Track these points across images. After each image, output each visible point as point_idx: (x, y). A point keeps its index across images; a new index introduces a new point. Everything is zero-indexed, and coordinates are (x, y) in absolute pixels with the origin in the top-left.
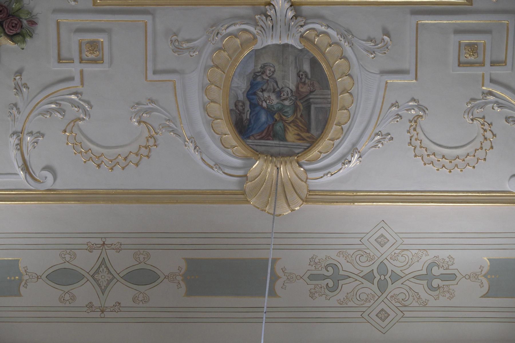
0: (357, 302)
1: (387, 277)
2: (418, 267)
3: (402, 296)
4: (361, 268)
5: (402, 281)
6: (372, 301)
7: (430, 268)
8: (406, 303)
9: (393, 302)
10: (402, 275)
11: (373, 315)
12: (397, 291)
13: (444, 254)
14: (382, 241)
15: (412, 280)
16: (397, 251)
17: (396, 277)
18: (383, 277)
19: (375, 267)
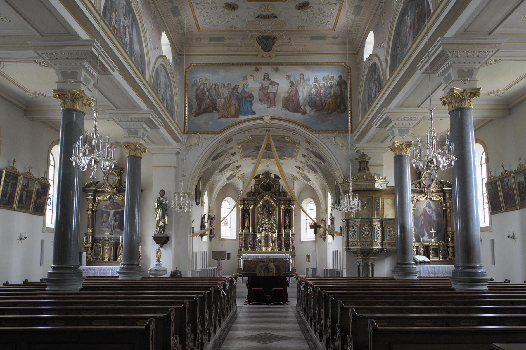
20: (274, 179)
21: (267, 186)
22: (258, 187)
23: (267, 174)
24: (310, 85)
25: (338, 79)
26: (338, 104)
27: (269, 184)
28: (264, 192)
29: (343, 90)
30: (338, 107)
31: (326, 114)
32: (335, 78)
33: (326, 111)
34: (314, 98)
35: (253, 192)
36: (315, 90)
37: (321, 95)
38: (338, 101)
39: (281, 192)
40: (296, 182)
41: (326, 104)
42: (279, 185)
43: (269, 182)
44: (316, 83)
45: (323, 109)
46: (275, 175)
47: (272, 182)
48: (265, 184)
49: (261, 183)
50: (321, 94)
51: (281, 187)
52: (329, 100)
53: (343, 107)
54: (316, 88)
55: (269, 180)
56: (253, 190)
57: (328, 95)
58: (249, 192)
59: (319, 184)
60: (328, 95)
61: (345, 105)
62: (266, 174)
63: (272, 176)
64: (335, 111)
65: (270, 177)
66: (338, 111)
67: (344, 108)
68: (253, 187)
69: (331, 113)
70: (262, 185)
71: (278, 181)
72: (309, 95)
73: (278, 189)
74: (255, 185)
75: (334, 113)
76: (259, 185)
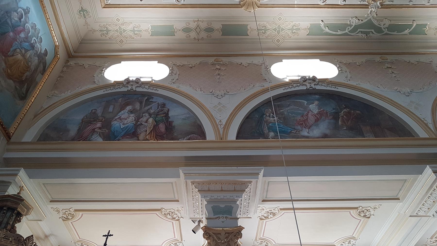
0: (271, 37)
1: (280, 30)
2: (290, 27)
3: (284, 35)
4: (273, 27)
5: (284, 30)
6: (275, 37)
7: (293, 27)
8: (285, 37)
9: (281, 37)
10: (285, 29)
11: (275, 41)
12: (283, 34)
13: (297, 23)
14: (280, 19)
15: (288, 30)
16: (284, 22)
17: (283, 29)
18: (279, 30)
19: (277, 27)
24: (17, 4)
25: (43, 52)
26: (24, 78)
29: (39, 70)
30: (21, 82)
31: (3, 69)
32: (42, 43)
33: (6, 64)
34: (8, 24)
36: (16, 19)
37: (18, 37)
38: (26, 74)
41: (13, 55)
44: (25, 14)
45: (5, 56)
50: (19, 34)
52: (19, 57)
53: (24, 90)
54: (20, 19)
57: (23, 51)
60: (23, 51)
61: (28, 90)
64: (14, 81)
66: (18, 87)
67: (24, 93)
69: (10, 77)
72: (7, 12)
75: (11, 81)
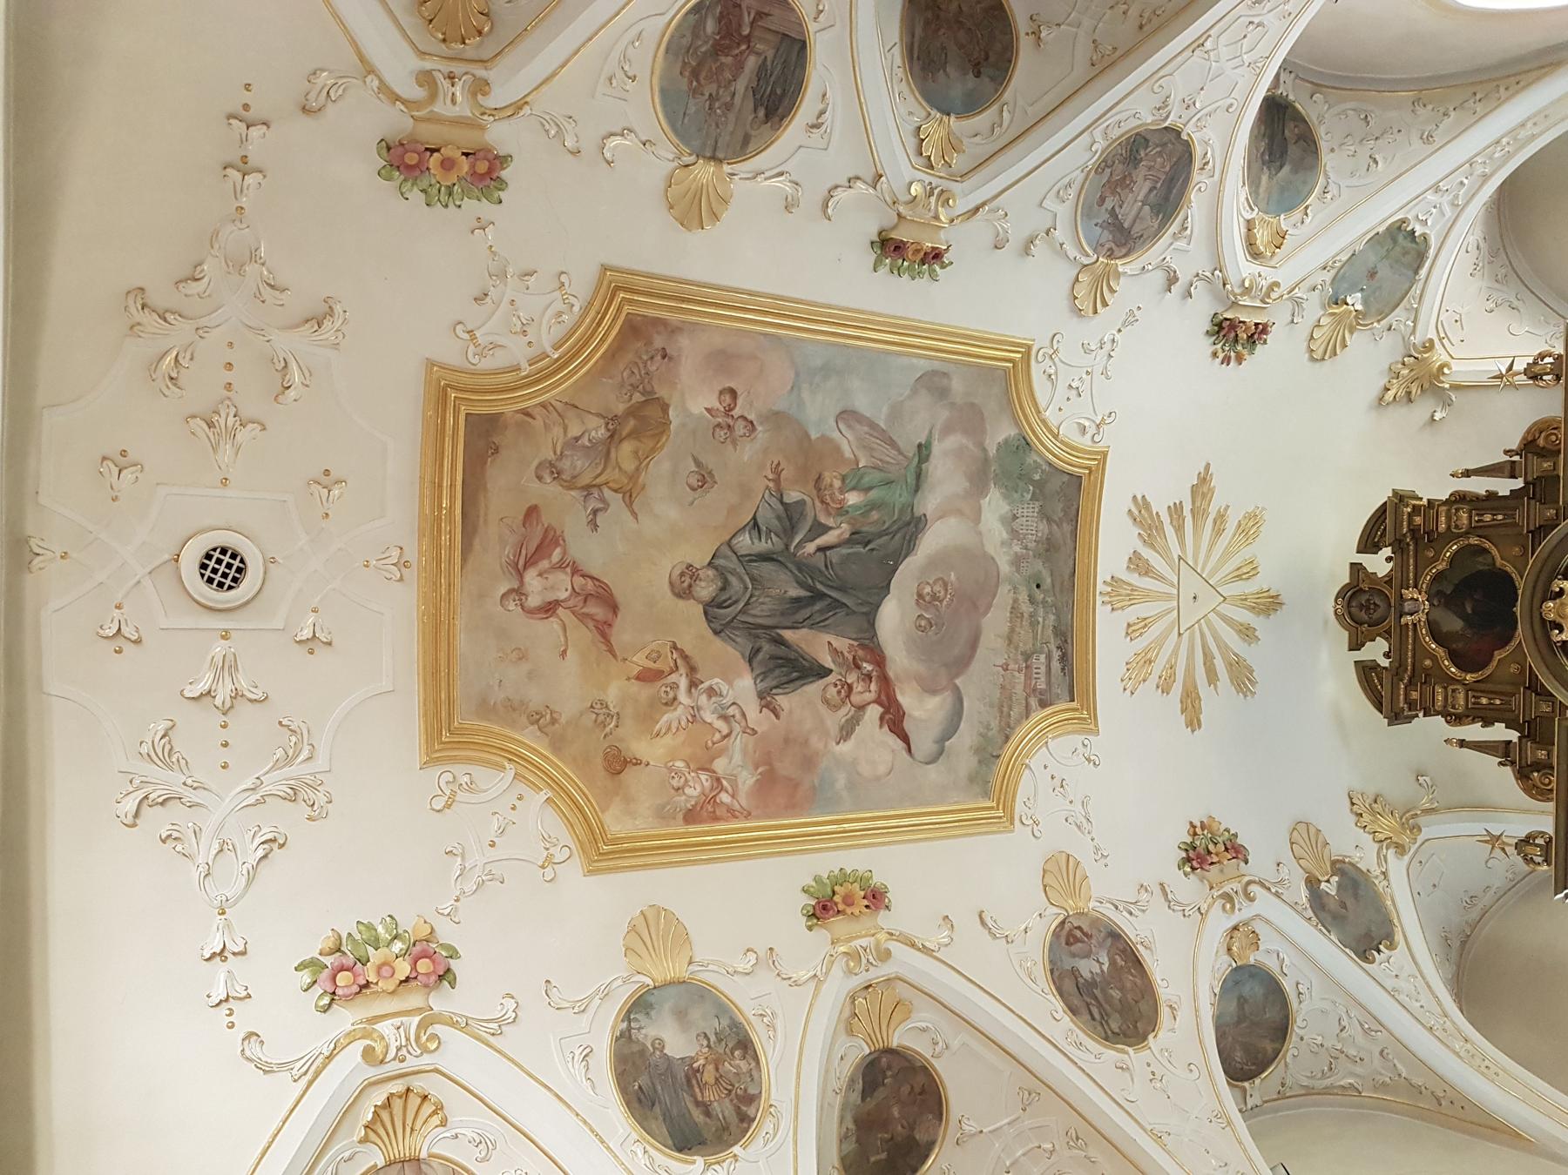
20: (1399, 546)
21: (1469, 610)
22: (1468, 688)
23: (1365, 607)
27: (1447, 594)
28: (1514, 643)
35: (1513, 736)
39: (1519, 483)
40: (1456, 366)
42: (1459, 499)
43: (1437, 595)
46: (1369, 543)
47: (1435, 559)
48: (1452, 623)
49: (1434, 658)
51: (1479, 486)
55: (1409, 593)
56: (1500, 732)
58: (1523, 775)
59: (1428, 139)
62: (1363, 616)
63: (1379, 564)
65: (1389, 580)
68: (1475, 732)
70: (1455, 658)
71: (1416, 509)
73: (1494, 511)
74: (1456, 719)
76: (1453, 680)
